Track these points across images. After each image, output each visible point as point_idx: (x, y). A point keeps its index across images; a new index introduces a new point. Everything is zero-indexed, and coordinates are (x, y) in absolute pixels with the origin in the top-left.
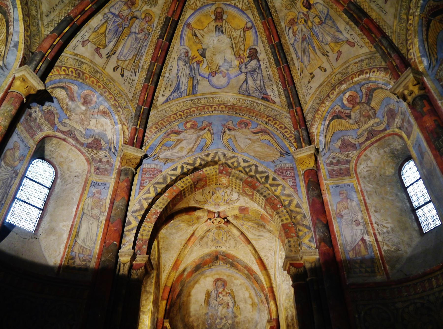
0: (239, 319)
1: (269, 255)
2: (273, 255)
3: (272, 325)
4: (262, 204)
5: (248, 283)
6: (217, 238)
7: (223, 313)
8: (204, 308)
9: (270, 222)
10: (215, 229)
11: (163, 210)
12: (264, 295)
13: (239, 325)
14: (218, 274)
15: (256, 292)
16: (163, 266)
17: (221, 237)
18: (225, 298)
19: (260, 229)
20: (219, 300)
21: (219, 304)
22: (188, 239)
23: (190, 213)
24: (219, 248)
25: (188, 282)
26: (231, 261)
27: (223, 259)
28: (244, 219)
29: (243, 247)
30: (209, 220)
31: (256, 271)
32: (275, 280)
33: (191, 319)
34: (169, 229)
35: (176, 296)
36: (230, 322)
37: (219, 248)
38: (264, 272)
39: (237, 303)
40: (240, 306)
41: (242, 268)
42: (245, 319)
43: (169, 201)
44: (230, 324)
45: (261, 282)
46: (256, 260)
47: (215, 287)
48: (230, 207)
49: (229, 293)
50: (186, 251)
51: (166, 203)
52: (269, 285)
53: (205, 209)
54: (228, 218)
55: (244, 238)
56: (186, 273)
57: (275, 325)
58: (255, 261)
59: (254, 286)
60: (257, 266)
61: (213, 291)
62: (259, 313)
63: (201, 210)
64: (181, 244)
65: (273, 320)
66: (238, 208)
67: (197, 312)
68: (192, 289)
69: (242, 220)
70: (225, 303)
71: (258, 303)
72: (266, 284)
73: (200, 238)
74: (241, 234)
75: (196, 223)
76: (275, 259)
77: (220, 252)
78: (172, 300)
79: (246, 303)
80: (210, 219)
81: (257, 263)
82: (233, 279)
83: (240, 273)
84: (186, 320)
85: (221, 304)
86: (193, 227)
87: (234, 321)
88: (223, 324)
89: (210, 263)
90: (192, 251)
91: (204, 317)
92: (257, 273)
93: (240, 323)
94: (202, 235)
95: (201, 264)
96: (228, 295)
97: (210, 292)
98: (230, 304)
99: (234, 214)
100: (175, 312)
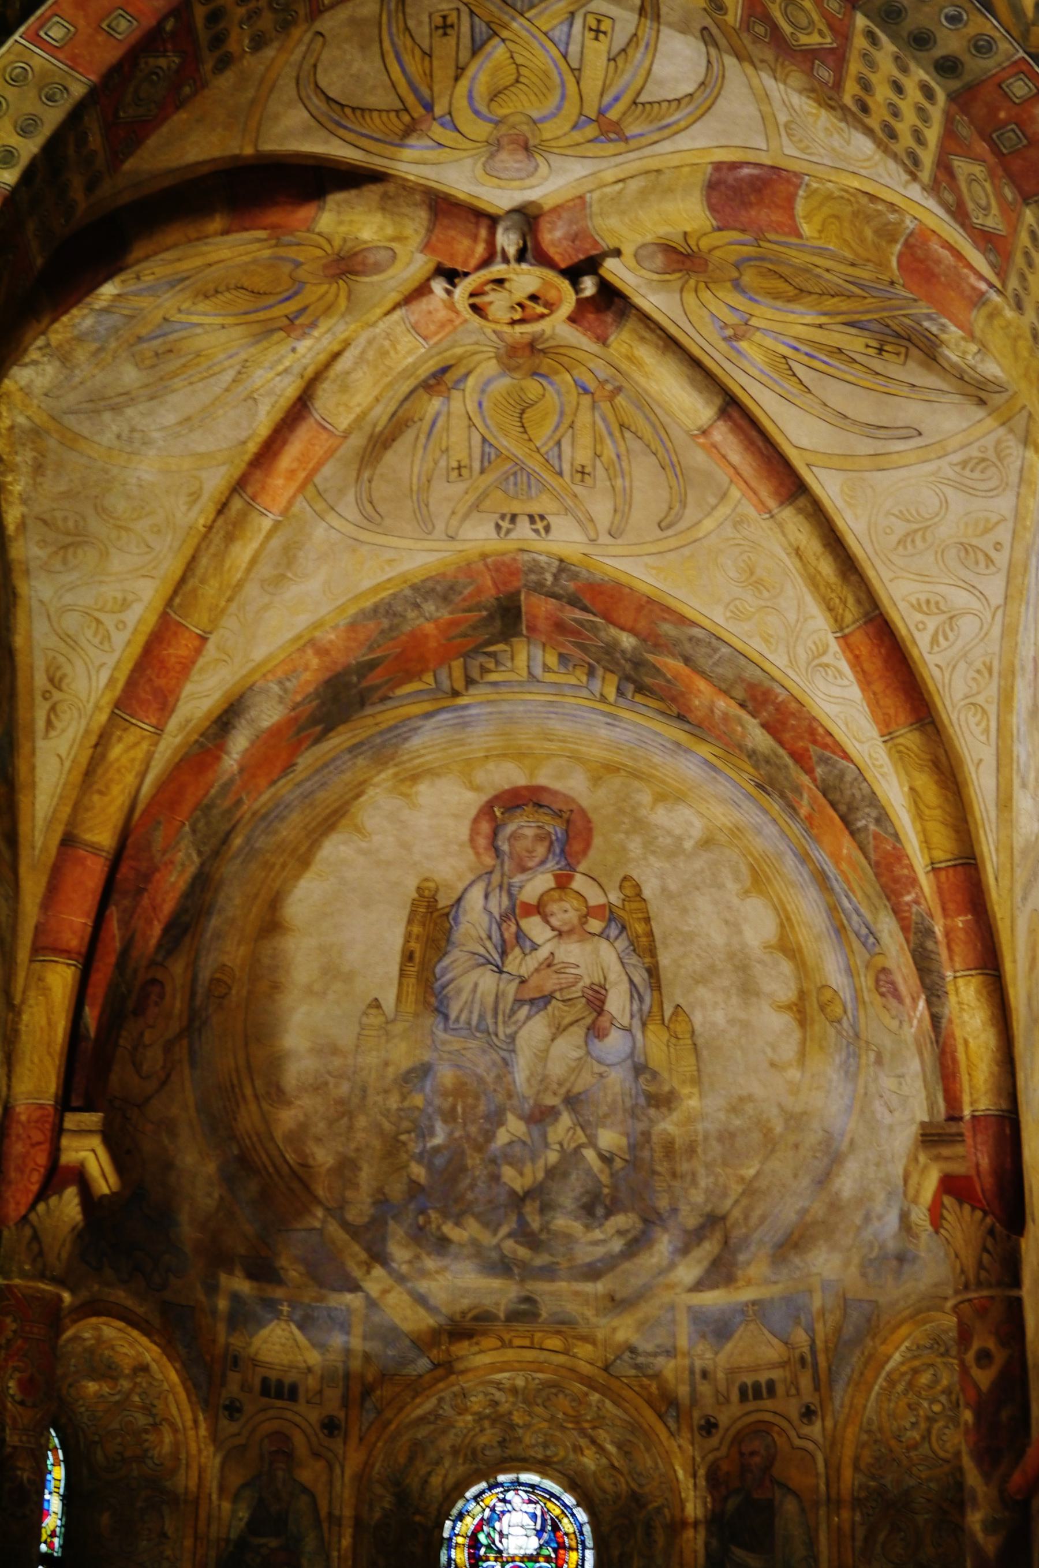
0: (690, 1120)
1: (961, 598)
2: (997, 599)
3: (958, 1168)
4: (919, 138)
5: (771, 830)
6: (509, 444)
7: (556, 1069)
8: (398, 1028)
9: (979, 300)
10: (491, 367)
11: (28, 176)
12: (905, 929)
13: (684, 1167)
14: (520, 755)
15: (833, 910)
16: (40, 680)
17: (542, 435)
18: (571, 952)
19: (892, 367)
20: (518, 963)
21: (519, 1002)
22: (252, 448)
23: (274, 216)
24: (524, 530)
25: (268, 818)
26: (627, 641)
27: (560, 627)
28: (748, 278)
29: (739, 522)
30: (439, 286)
31: (841, 734)
32: (1005, 803)
33: (287, 1118)
34: (81, 355)
35: (157, 930)
36: (609, 1138)
37: (524, 530)
38: (910, 739)
39: (675, 995)
40: (697, 1018)
41: (723, 704)
42: (738, 1123)
43: (78, 90)
44: (607, 1159)
45: (883, 818)
46: (845, 640)
47: (489, 860)
48: (633, 162)
49: (609, 914)
50: (242, 553)
51: (53, 117)
52: (944, 847)
53: (407, 188)
54: (611, 267)
55: (749, 445)
56: (239, 743)
57: (985, 1162)
58: (834, 647)
59: (820, 856)
60: (855, 692)
61: (476, 895)
62: (851, 1075)
63: (373, 191)
64: (195, 497)
65: (965, 1127)
66: (700, 178)
67: (337, 1062)
68: (297, 877)
69: (737, 285)
70: (576, 992)
71: (847, 995)
72: (927, 843)
73: (357, 440)
74: (723, 413)
75: (328, 310)
76: (1010, 631)
77: (536, 568)
78: (121, 964)
79: (748, 990)
80: (452, 276)
81: (856, 662)
82: (645, 797)
83: (705, 750)
84: (248, 1118)
85: (542, 1001)
86: (304, 346)
87: (647, 1135)
88: (553, 1157)
89: (445, 658)
90: (289, 555)
91: (393, 1102)
92: (852, 747)
93: (691, 1150)
94: (381, 414)
95: (371, 666)
96: (595, 925)
97: (444, 901)
98: (618, 1003)
99: (663, 230)
100: (153, 1058)
